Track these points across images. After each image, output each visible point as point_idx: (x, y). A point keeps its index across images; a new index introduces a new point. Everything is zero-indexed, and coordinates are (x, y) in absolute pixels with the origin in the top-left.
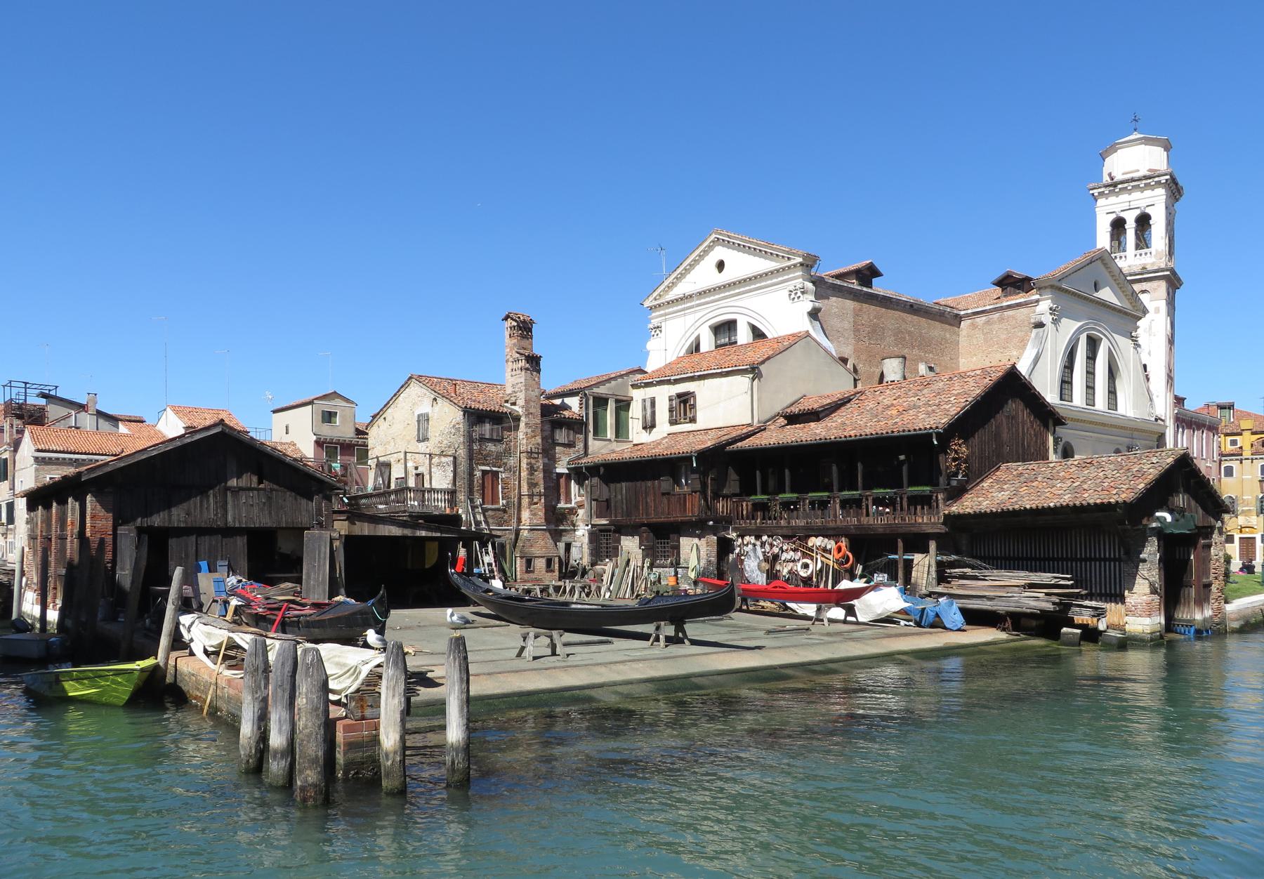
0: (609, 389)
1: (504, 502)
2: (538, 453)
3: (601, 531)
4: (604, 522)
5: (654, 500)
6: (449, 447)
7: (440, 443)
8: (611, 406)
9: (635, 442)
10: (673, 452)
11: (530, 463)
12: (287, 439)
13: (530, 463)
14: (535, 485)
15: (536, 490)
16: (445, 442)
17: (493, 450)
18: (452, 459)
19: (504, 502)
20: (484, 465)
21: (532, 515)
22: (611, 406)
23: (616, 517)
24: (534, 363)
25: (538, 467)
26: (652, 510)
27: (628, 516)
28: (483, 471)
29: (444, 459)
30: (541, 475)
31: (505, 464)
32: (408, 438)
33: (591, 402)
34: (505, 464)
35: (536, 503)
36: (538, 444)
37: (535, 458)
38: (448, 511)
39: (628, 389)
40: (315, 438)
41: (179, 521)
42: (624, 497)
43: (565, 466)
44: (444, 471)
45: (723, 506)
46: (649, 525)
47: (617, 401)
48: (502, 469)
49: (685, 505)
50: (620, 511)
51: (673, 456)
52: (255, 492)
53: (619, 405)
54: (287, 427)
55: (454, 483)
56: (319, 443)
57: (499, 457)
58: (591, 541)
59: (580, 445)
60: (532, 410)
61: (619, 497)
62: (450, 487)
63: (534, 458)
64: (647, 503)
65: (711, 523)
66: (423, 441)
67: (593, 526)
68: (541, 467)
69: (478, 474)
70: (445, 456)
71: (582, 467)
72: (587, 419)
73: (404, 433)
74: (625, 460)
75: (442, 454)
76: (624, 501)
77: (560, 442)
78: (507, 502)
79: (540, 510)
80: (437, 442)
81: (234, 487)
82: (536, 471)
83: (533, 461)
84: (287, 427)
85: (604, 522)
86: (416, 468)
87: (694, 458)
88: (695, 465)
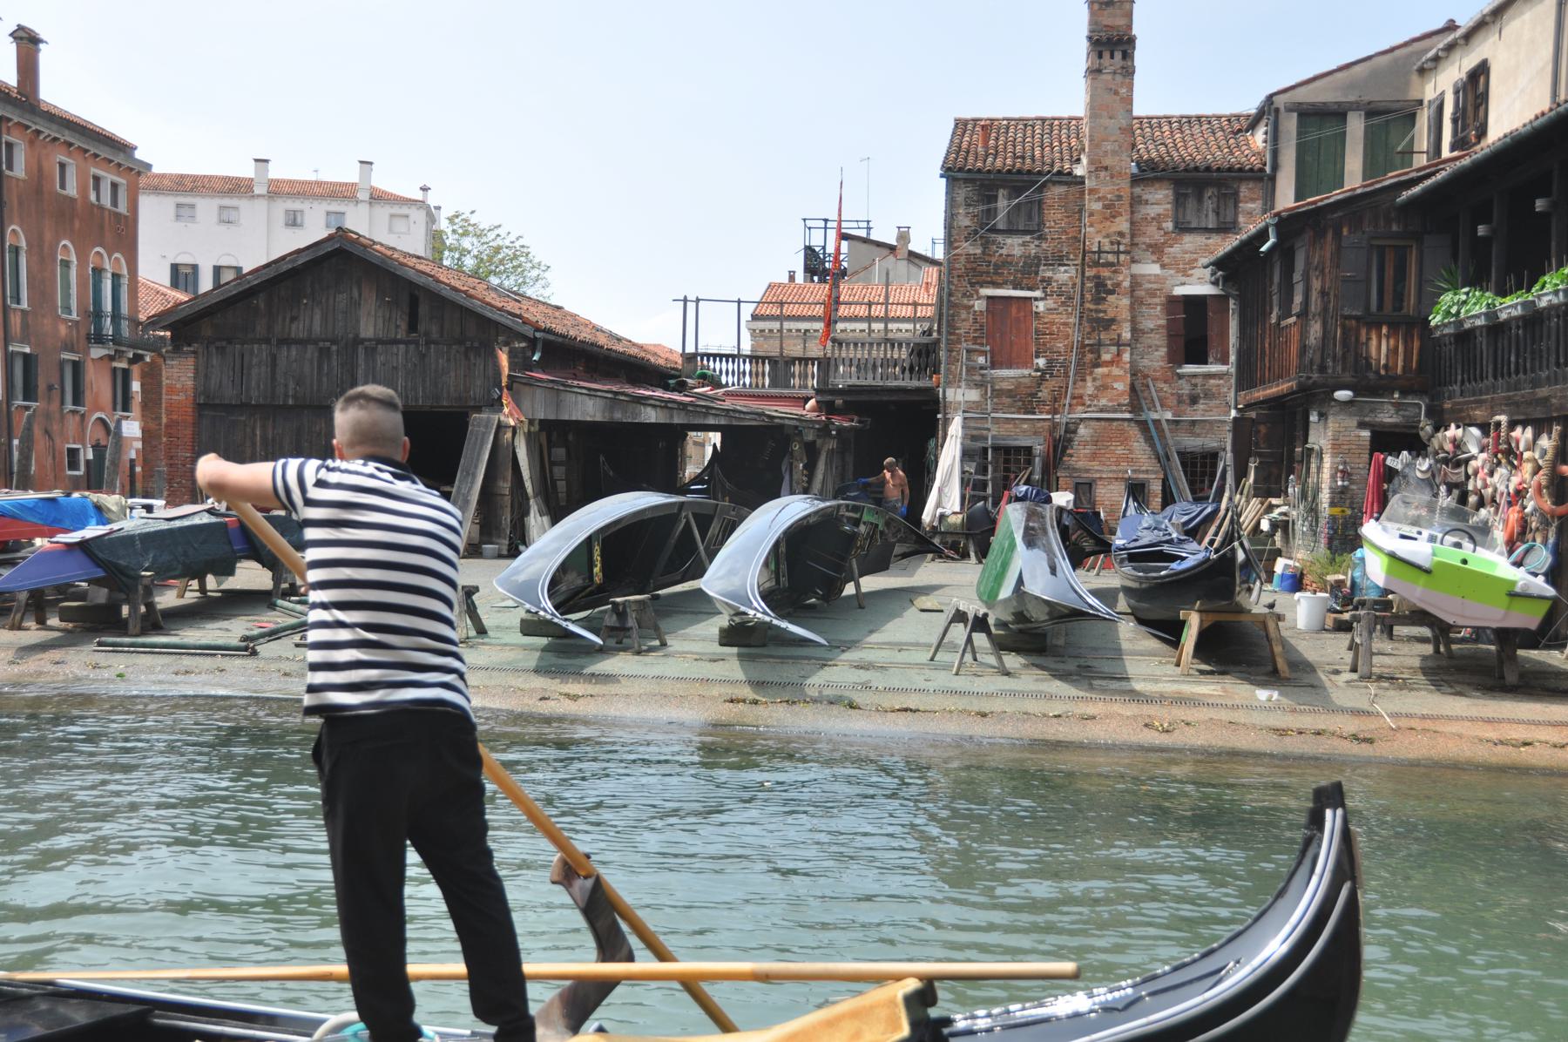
0: (1352, 86)
1: (1041, 362)
2: (1118, 253)
8: (1356, 126)
11: (1097, 277)
13: (1097, 277)
17: (1017, 251)
20: (996, 285)
22: (1356, 126)
24: (1118, 55)
25: (1118, 285)
28: (989, 298)
30: (1126, 301)
33: (1290, 124)
34: (1048, 281)
36: (1121, 234)
37: (1111, 264)
39: (1407, 84)
41: (286, 396)
45: (1393, 352)
47: (1371, 112)
48: (1038, 294)
52: (402, 347)
53: (1376, 120)
60: (1107, 162)
65: (1343, 395)
68: (1126, 284)
69: (979, 305)
72: (1275, 167)
77: (1193, 225)
78: (1050, 362)
81: (370, 340)
82: (1112, 292)
83: (1105, 273)
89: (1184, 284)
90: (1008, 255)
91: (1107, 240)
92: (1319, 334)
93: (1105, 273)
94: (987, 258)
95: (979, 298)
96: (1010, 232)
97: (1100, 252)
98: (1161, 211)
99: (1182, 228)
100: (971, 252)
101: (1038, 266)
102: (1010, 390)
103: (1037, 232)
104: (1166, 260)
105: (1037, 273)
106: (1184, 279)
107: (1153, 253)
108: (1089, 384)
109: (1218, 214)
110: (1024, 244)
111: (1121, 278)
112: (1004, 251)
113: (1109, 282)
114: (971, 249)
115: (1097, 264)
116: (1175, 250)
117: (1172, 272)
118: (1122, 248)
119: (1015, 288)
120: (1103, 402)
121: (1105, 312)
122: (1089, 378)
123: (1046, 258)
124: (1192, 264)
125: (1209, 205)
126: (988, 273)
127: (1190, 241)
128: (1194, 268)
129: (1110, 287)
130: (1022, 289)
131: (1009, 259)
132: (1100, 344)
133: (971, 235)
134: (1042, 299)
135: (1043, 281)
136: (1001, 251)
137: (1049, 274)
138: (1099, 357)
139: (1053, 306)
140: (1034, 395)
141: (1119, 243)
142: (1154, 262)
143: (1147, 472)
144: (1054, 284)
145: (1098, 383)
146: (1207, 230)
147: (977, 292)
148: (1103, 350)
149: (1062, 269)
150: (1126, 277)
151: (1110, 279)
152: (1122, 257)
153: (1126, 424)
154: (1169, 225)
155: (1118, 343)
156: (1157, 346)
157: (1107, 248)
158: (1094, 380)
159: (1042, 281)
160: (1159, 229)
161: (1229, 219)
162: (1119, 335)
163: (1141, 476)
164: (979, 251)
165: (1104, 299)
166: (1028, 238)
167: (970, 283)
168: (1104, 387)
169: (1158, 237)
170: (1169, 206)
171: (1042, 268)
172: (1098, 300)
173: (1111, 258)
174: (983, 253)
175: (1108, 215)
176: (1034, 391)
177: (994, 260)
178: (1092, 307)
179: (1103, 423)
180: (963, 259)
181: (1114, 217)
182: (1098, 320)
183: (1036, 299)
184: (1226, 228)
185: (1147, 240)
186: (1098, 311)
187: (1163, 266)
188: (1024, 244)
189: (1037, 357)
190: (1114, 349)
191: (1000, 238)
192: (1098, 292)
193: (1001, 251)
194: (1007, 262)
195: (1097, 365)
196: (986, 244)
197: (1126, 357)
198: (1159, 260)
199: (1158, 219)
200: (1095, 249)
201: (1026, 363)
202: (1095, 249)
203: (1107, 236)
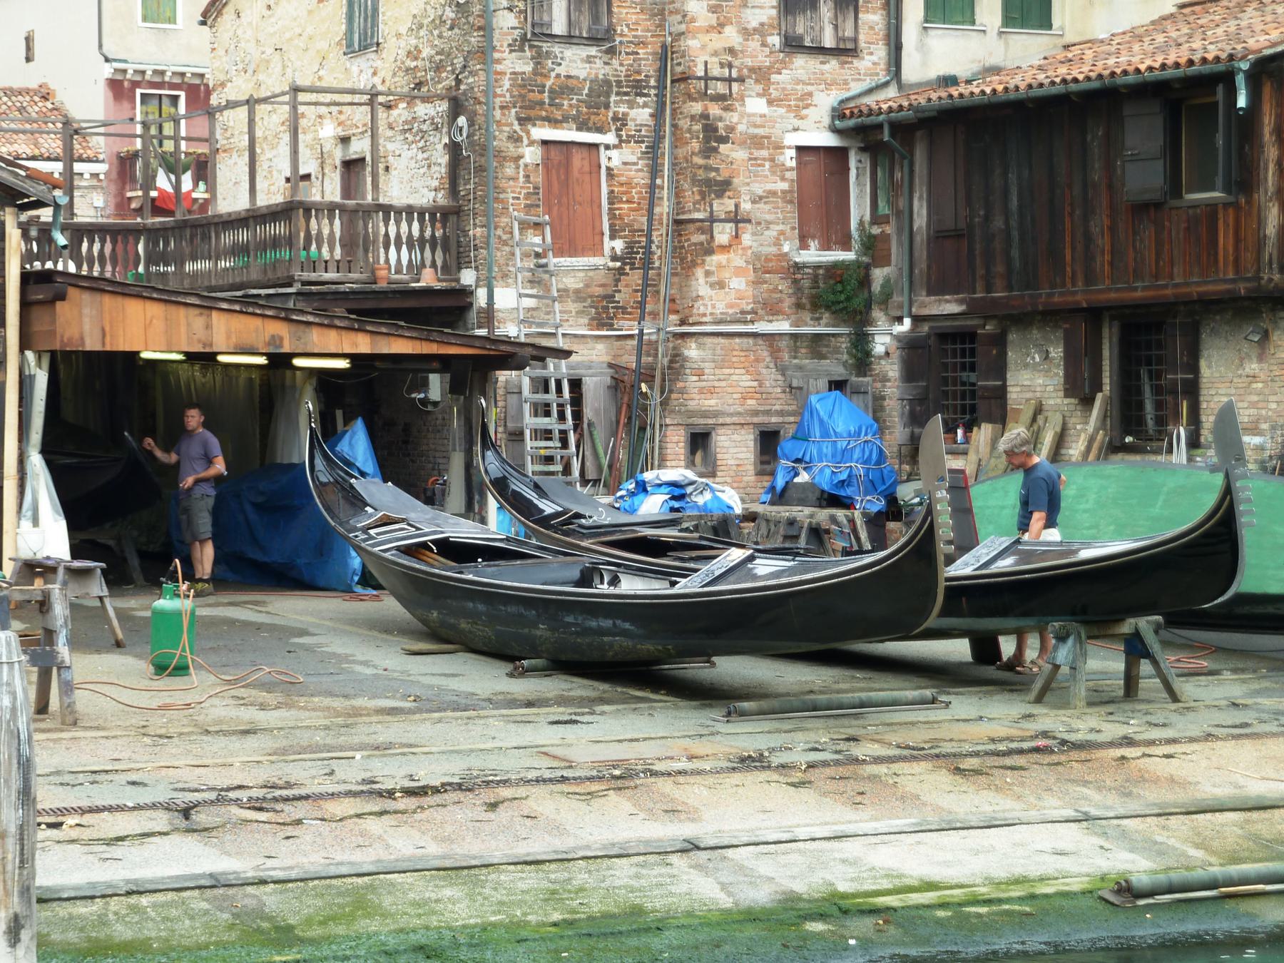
1: (619, 245)
3: (944, 337)
4: (950, 306)
5: (1113, 229)
6: (439, 68)
7: (414, 54)
9: (1070, 38)
10: (1171, 59)
11: (705, 116)
12: (28, 77)
13: (705, 116)
14: (722, 187)
15: (723, 206)
16: (426, 52)
18: (444, 106)
19: (619, 245)
20: (553, 122)
21: (712, 286)
23: (989, 289)
25: (731, 129)
26: (1102, 261)
27: (1028, 287)
28: (545, 143)
29: (422, 110)
31: (621, 121)
32: (322, 45)
35: (725, 248)
36: (731, 51)
37: (720, 98)
38: (428, 279)
40: (107, 71)
42: (1014, 223)
43: (826, 121)
44: (423, 150)
46: (1095, 315)
48: (610, 138)
49: (1213, 242)
50: (1000, 268)
51: (1169, 73)
54: (29, 40)
55: (453, 190)
56: (119, 88)
57: (601, 92)
58: (910, 373)
59: (874, 57)
61: (998, 223)
62: (442, 199)
63: (720, 98)
64: (1088, 238)
66: (364, 48)
67: (917, 320)
69: (531, 155)
70: (426, 100)
71: (879, 126)
73: (310, 30)
74: (1012, 96)
75: (418, 92)
76: (1015, 234)
78: (630, 247)
79: (738, 272)
80: (402, 53)
82: (724, 140)
83: (714, 110)
84: (29, 40)
85: (950, 306)
86: (345, 140)
87: (1240, 80)
88: (1242, 102)
89: (796, 130)
90: (568, 77)
91: (716, 60)
92: (1275, 222)
93: (714, 110)
94: (539, 79)
95: (531, 143)
96: (569, 39)
97: (707, 78)
98: (764, 19)
99: (793, 45)
100: (518, 69)
101: (608, 95)
102: (577, 291)
103: (602, 38)
104: (774, 94)
105: (607, 106)
106: (797, 123)
107: (757, 81)
108: (702, 280)
109: (836, 27)
110: (589, 60)
111: (735, 120)
112: (562, 70)
113: (720, 125)
114: (514, 64)
115: (704, 95)
116: (783, 78)
117: (782, 111)
118: (735, 74)
119: (579, 129)
120: (720, 308)
121: (717, 170)
122: (699, 272)
123: (619, 83)
124: (805, 101)
125: (826, 11)
126: (542, 103)
127: (803, 65)
128: (807, 106)
129: (722, 132)
130: (589, 130)
131: (571, 83)
132: (712, 219)
133: (521, 44)
134: (615, 147)
135: (615, 119)
136: (558, 70)
137: (622, 109)
138: (712, 237)
139: (633, 159)
140: (610, 298)
141: (730, 66)
142: (759, 95)
143: (781, 413)
144: (631, 125)
145: (713, 279)
146: (820, 50)
147: (528, 133)
148: (717, 227)
149: (640, 100)
150: (742, 115)
151: (721, 119)
152: (735, 86)
153: (751, 341)
154: (775, 40)
155: (737, 219)
156: (769, 223)
157: (716, 71)
158: (708, 274)
159: (615, 119)
160: (764, 45)
161: (849, 33)
162: (737, 206)
163: (774, 420)
164: (528, 68)
165: (715, 150)
166: (593, 51)
167: (522, 121)
168: (721, 285)
169: (763, 59)
170: (774, 12)
171: (613, 98)
172: (709, 151)
173: (721, 88)
174: (535, 72)
175: (714, 23)
176: (609, 291)
177: (548, 84)
178: (698, 160)
179: (721, 340)
180: (507, 84)
181: (721, 25)
182: (708, 183)
183: (607, 147)
184: (846, 51)
185: (749, 62)
186: (708, 168)
187: (770, 102)
188: (589, 60)
189: (612, 237)
190: (729, 227)
191: (557, 49)
192: (707, 140)
193: (558, 70)
194: (566, 88)
195: (710, 251)
196: (539, 58)
197: (747, 239)
198: (765, 93)
199: (761, 31)
200: (701, 73)
201: (597, 249)
202: (701, 73)
203: (715, 54)
